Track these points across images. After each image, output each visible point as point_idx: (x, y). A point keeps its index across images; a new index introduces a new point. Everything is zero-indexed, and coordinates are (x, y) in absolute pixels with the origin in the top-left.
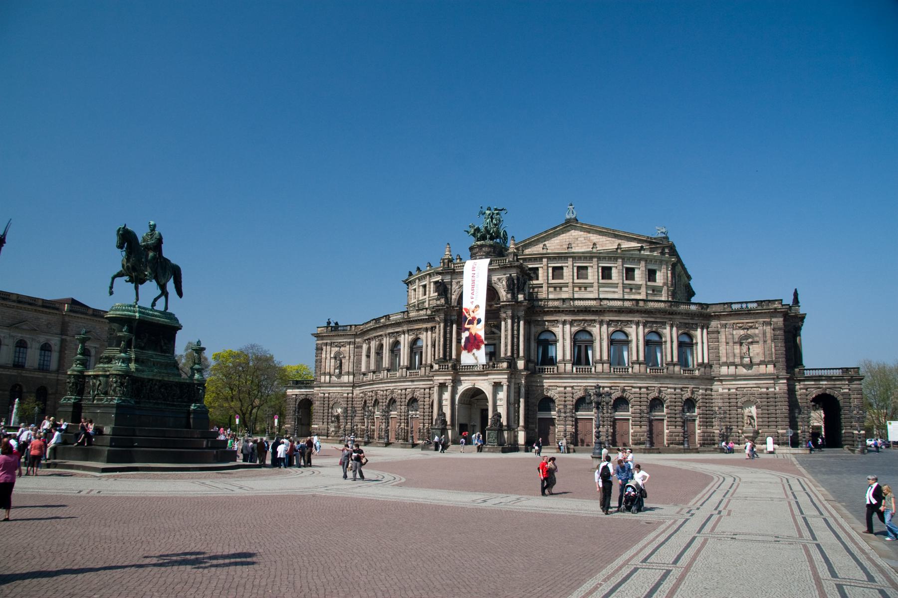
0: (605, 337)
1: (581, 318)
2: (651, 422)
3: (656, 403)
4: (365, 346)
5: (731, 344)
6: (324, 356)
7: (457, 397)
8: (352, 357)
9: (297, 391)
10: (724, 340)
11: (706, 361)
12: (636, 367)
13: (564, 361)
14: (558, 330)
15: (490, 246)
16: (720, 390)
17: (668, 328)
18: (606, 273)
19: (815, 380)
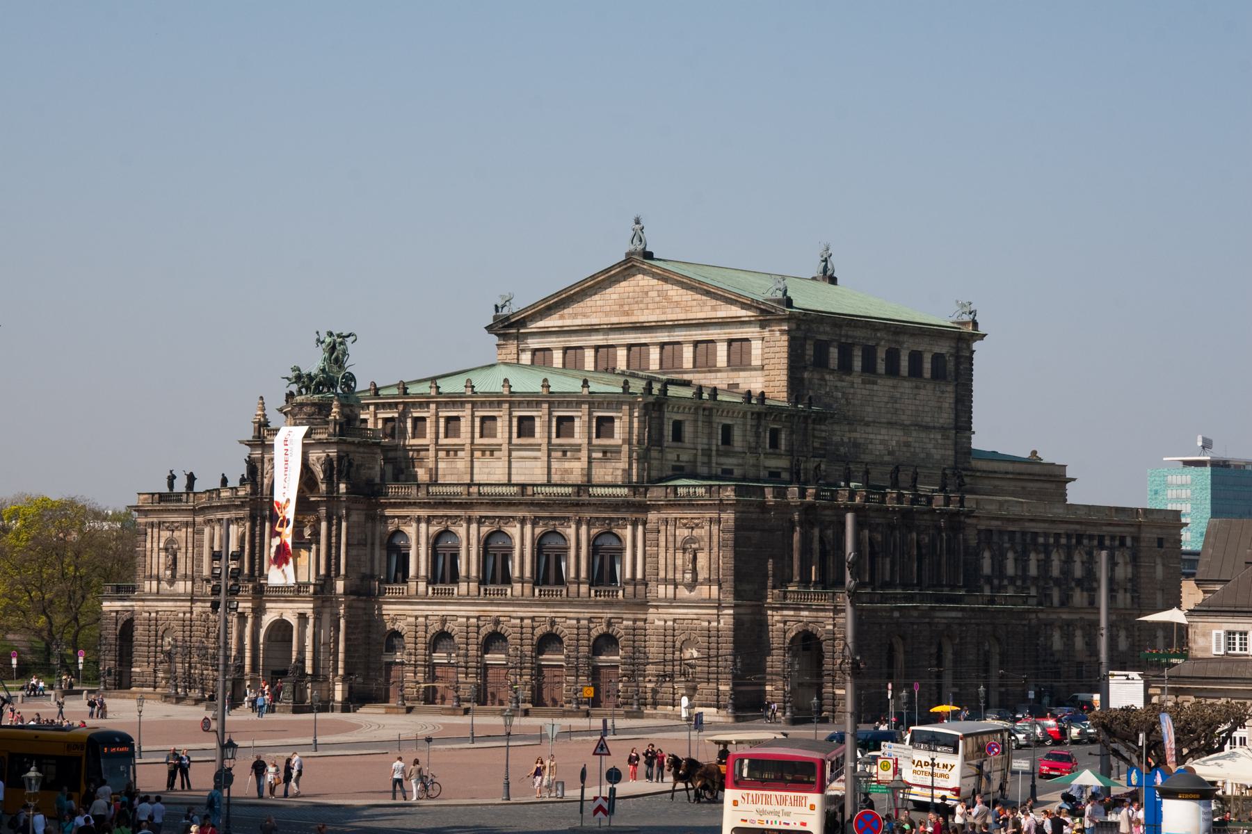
0: (474, 541)
1: (441, 513)
2: (539, 670)
3: (549, 640)
4: (207, 530)
5: (671, 551)
6: (149, 545)
7: (262, 632)
8: (190, 549)
9: (117, 605)
10: (662, 544)
11: (639, 575)
12: (517, 587)
13: (417, 576)
14: (410, 530)
15: (313, 404)
16: (657, 623)
17: (574, 526)
18: (525, 428)
19: (795, 609)
